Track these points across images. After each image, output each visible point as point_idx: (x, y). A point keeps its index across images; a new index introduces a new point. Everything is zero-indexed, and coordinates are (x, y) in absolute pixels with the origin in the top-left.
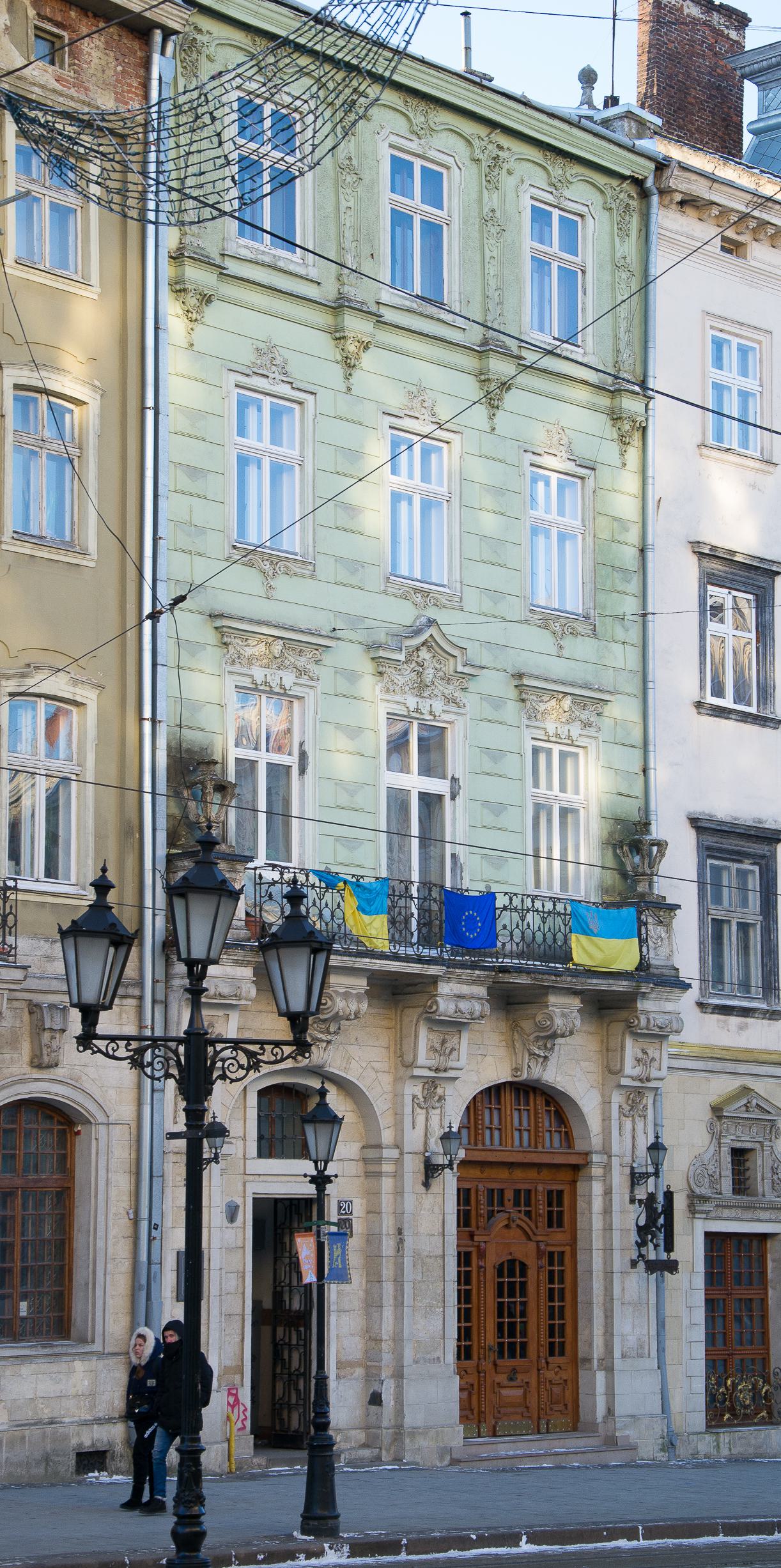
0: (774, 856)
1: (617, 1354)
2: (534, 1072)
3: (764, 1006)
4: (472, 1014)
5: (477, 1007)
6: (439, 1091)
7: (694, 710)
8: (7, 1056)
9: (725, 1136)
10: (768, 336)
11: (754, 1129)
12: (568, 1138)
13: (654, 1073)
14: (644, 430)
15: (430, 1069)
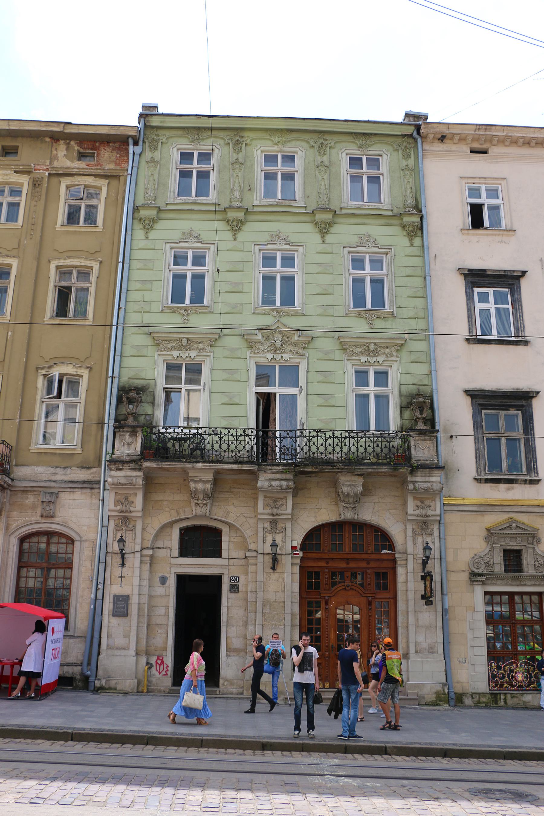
0: (530, 406)
1: (412, 650)
2: (349, 515)
3: (528, 478)
4: (281, 486)
5: (284, 483)
6: (280, 525)
7: (467, 343)
8: (30, 513)
9: (497, 543)
10: (505, 181)
11: (519, 540)
12: (391, 547)
13: (430, 512)
14: (421, 228)
15: (268, 514)
